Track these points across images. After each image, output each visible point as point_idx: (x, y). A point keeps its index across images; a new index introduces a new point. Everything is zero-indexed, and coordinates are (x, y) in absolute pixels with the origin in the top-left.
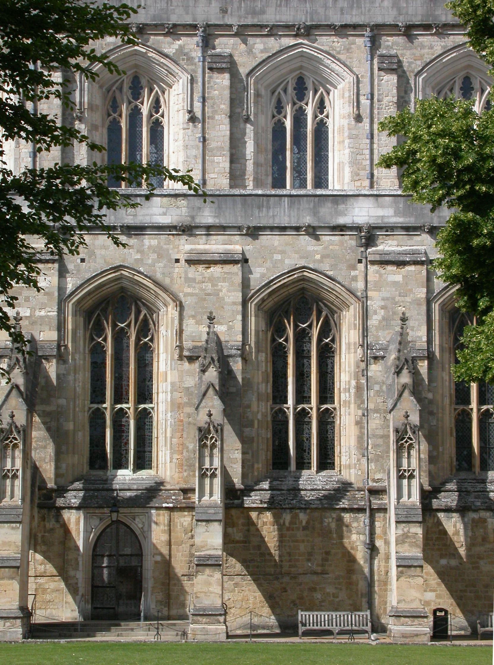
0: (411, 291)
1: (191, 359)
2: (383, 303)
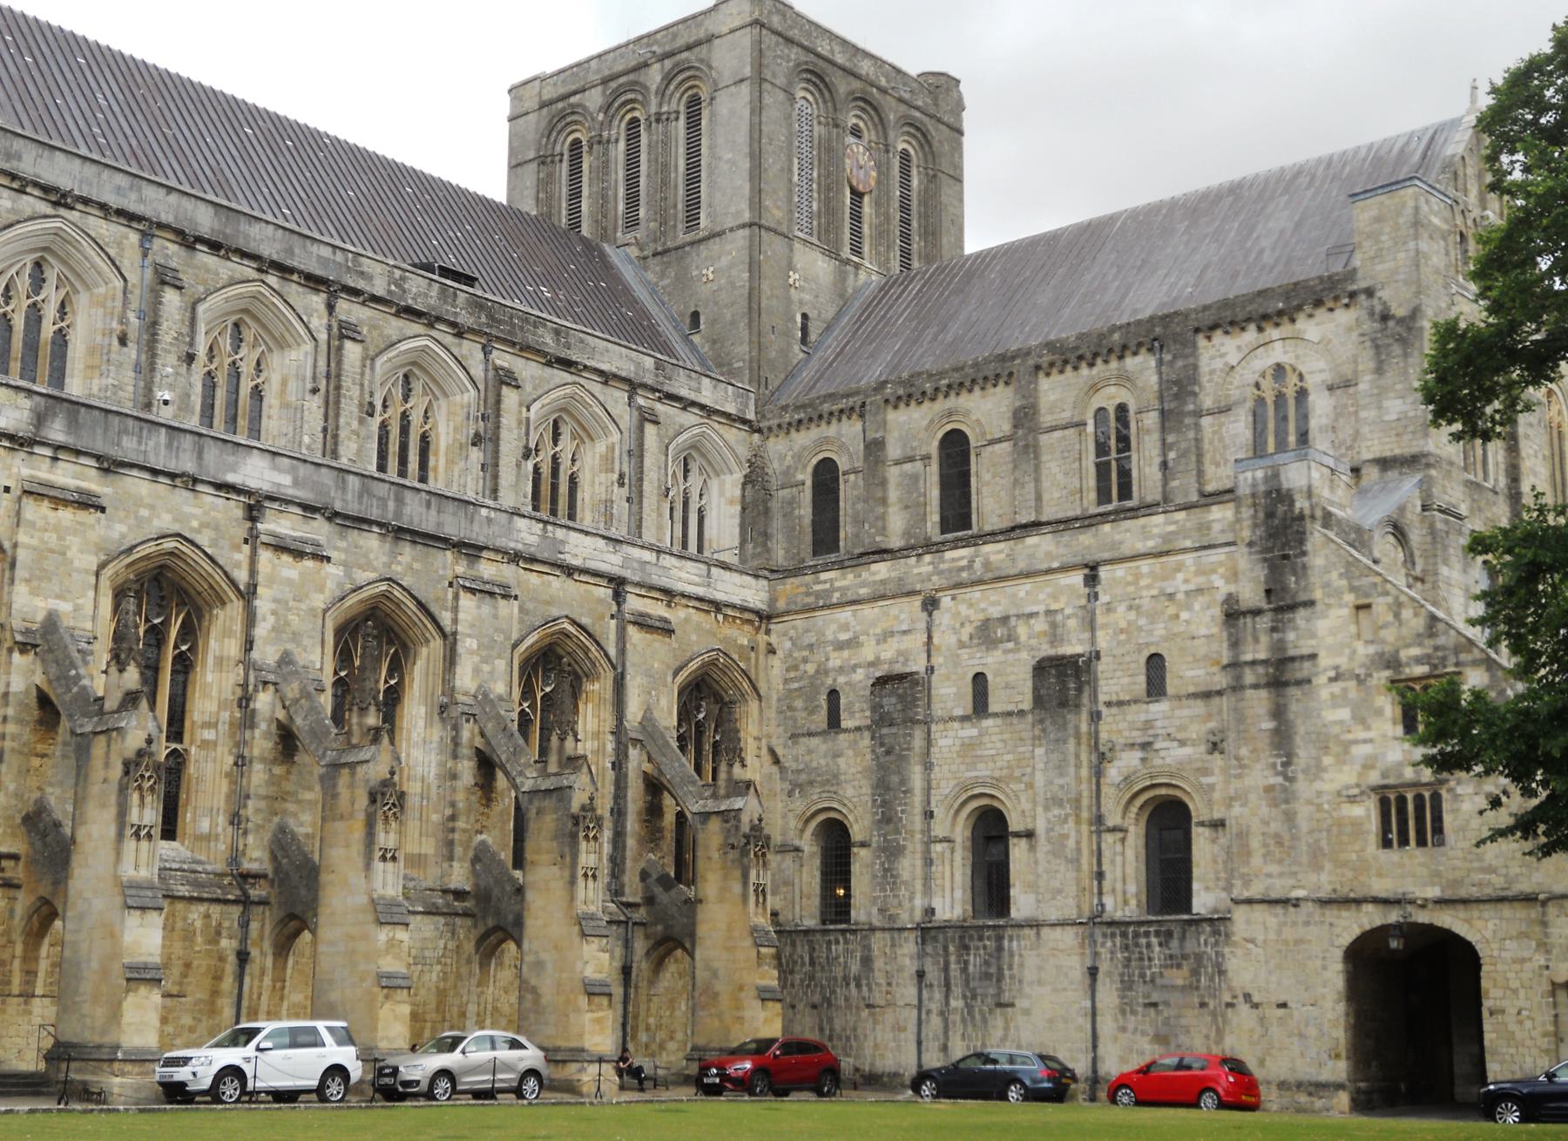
0: (307, 596)
1: (24, 648)
2: (274, 606)
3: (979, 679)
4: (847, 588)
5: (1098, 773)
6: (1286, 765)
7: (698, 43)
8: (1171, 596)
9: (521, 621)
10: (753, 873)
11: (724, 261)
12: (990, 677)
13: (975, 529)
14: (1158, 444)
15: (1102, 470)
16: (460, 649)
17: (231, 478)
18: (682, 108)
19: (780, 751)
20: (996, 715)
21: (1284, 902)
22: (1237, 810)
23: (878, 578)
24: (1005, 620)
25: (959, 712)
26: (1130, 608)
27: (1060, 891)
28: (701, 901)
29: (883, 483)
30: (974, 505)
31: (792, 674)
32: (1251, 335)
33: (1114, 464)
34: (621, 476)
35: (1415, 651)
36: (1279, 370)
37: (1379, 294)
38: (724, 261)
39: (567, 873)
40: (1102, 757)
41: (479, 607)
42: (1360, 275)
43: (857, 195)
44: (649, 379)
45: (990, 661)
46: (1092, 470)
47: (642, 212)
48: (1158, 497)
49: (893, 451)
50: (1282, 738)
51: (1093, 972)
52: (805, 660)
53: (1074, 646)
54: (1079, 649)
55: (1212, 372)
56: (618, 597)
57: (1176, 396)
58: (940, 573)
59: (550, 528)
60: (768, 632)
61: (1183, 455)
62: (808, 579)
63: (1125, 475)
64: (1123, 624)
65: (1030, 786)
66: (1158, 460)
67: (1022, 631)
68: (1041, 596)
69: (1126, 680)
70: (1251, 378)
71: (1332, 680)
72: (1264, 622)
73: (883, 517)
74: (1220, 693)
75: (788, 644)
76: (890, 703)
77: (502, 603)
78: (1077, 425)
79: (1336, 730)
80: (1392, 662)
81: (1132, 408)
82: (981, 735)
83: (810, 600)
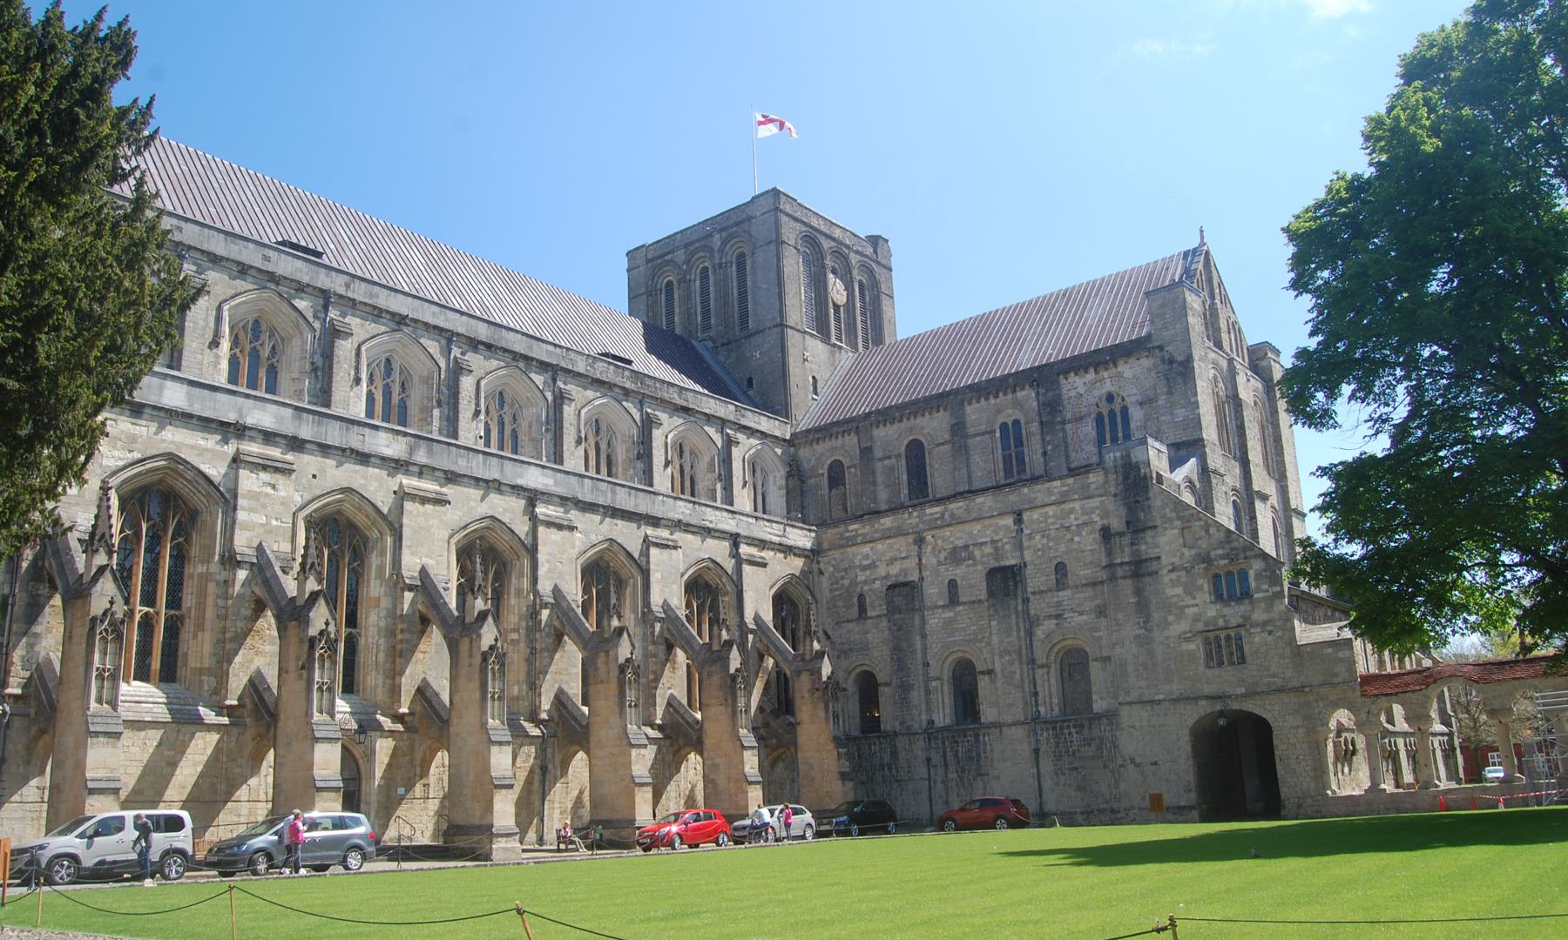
3: (952, 584)
4: (867, 534)
5: (1030, 634)
6: (1146, 622)
7: (742, 222)
8: (1068, 528)
9: (684, 562)
10: (831, 705)
11: (766, 347)
12: (959, 582)
13: (931, 497)
14: (1040, 442)
15: (1007, 459)
16: (652, 579)
17: (520, 482)
18: (734, 260)
19: (830, 633)
20: (965, 603)
21: (1152, 702)
22: (1118, 650)
23: (885, 527)
24: (966, 547)
25: (941, 603)
26: (1043, 536)
27: (1012, 705)
28: (799, 724)
29: (873, 472)
30: (929, 483)
31: (835, 586)
32: (1091, 375)
33: (1013, 454)
34: (720, 475)
35: (1220, 552)
36: (1110, 398)
37: (1167, 349)
38: (766, 347)
39: (730, 710)
40: (1031, 623)
41: (661, 553)
42: (1154, 337)
43: (836, 307)
44: (732, 418)
45: (958, 572)
46: (1001, 458)
47: (713, 321)
48: (1043, 472)
49: (878, 453)
50: (1142, 607)
51: (1037, 751)
52: (843, 578)
53: (1011, 562)
54: (1013, 562)
55: (1070, 398)
56: (736, 545)
57: (1049, 413)
58: (923, 522)
59: (696, 506)
60: (818, 563)
61: (1056, 447)
62: (842, 529)
63: (1021, 461)
64: (1040, 546)
65: (989, 644)
66: (1041, 451)
67: (977, 553)
68: (988, 533)
69: (1044, 578)
70: (1094, 401)
71: (1170, 571)
72: (1126, 540)
73: (874, 492)
74: (1102, 583)
75: (831, 569)
76: (899, 601)
77: (673, 551)
78: (989, 432)
79: (1175, 599)
80: (1206, 559)
81: (1022, 422)
82: (955, 616)
83: (844, 542)
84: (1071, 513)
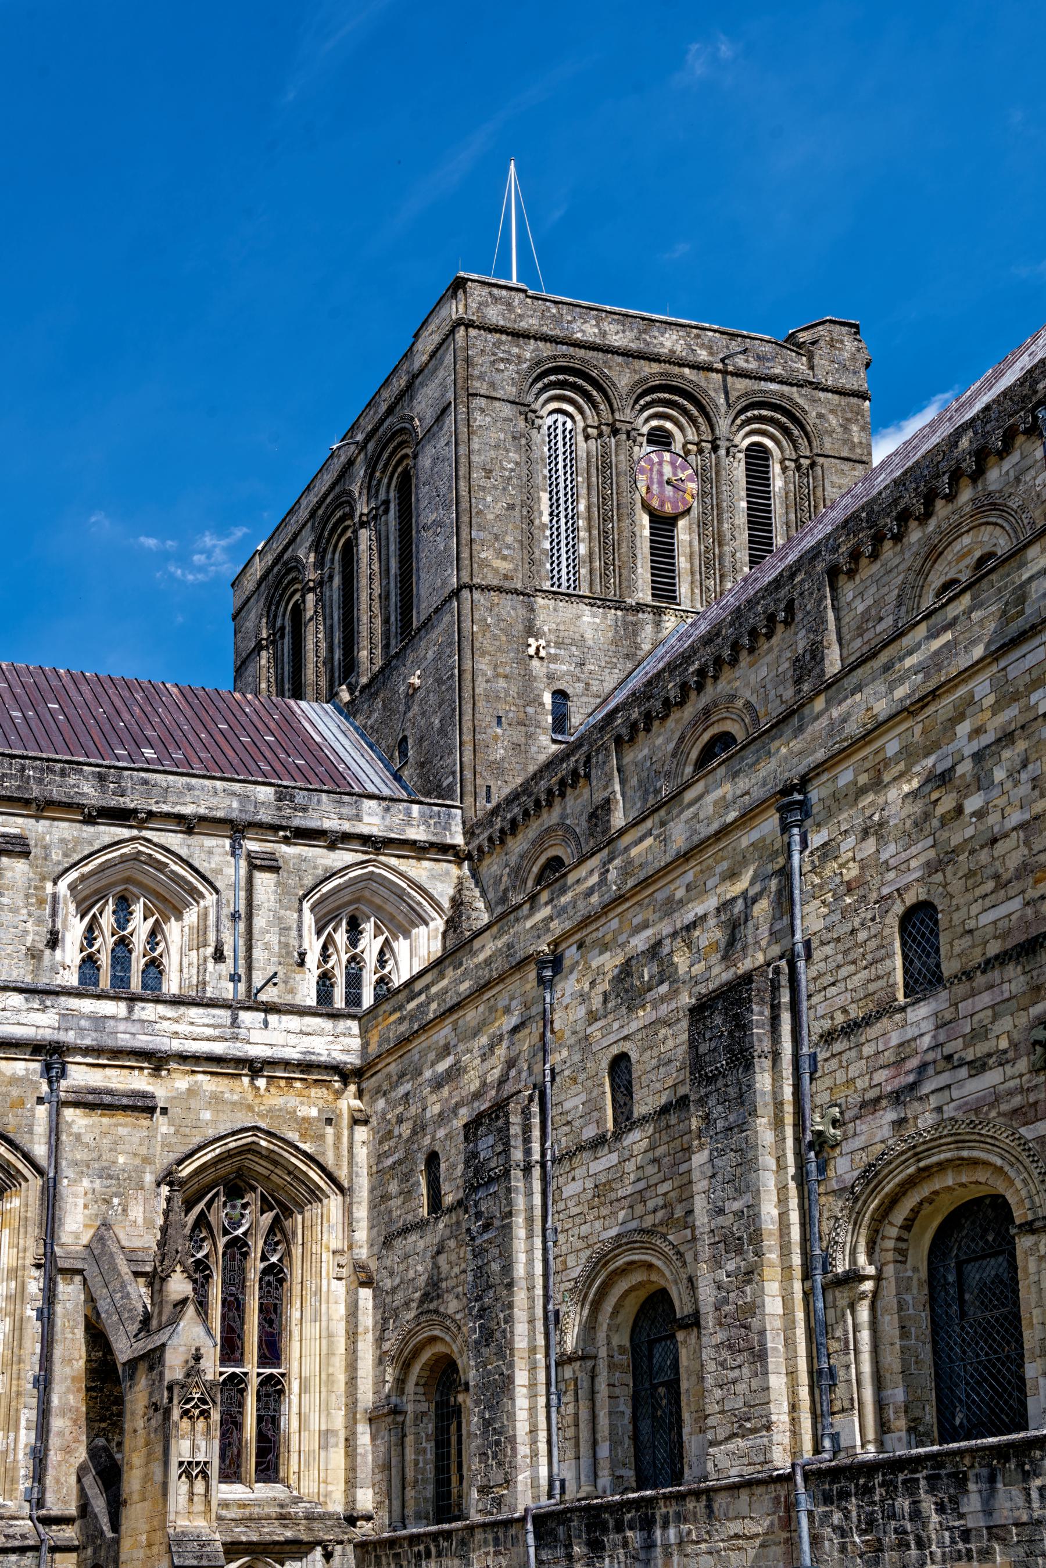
12: (634, 1056)
84: (961, 717)
